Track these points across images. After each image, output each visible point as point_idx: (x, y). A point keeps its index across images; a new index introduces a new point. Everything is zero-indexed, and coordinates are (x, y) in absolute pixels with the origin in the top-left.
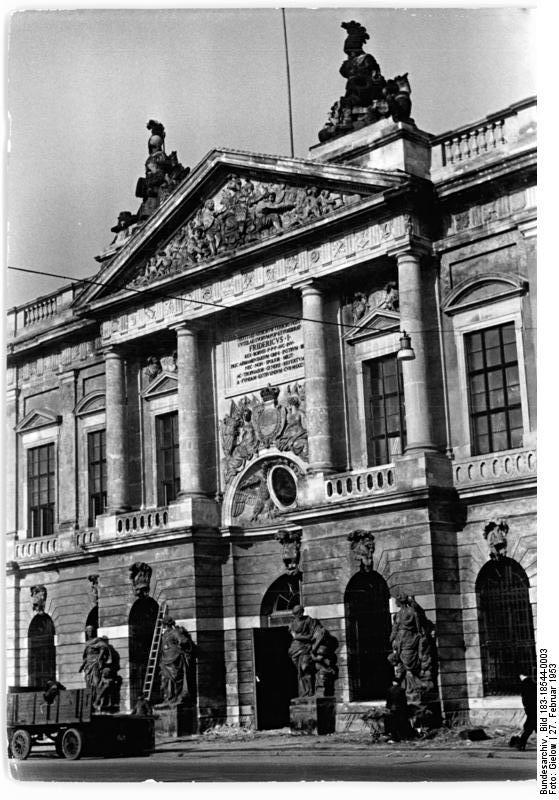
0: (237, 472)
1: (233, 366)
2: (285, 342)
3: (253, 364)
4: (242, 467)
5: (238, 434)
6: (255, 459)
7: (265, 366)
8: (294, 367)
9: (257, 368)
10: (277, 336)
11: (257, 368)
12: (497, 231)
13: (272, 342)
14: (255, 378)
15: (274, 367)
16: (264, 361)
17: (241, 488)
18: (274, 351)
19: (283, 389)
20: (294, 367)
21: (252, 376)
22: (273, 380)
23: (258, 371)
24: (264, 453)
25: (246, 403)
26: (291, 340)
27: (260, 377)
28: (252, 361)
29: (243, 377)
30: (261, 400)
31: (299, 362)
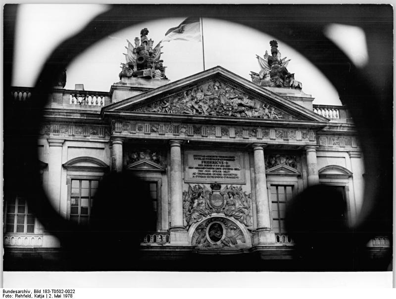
0: (198, 221)
1: (190, 168)
2: (225, 164)
3: (204, 170)
4: (201, 219)
5: (194, 203)
6: (209, 217)
7: (212, 173)
8: (230, 177)
9: (206, 173)
10: (220, 161)
11: (206, 173)
12: (339, 150)
13: (223, 163)
14: (205, 177)
15: (217, 174)
16: (212, 170)
17: (197, 229)
18: (217, 167)
19: (223, 187)
20: (230, 177)
21: (203, 175)
22: (218, 180)
23: (207, 174)
24: (214, 215)
25: (199, 188)
26: (228, 165)
27: (208, 177)
28: (203, 168)
29: (197, 175)
30: (210, 189)
31: (233, 176)
